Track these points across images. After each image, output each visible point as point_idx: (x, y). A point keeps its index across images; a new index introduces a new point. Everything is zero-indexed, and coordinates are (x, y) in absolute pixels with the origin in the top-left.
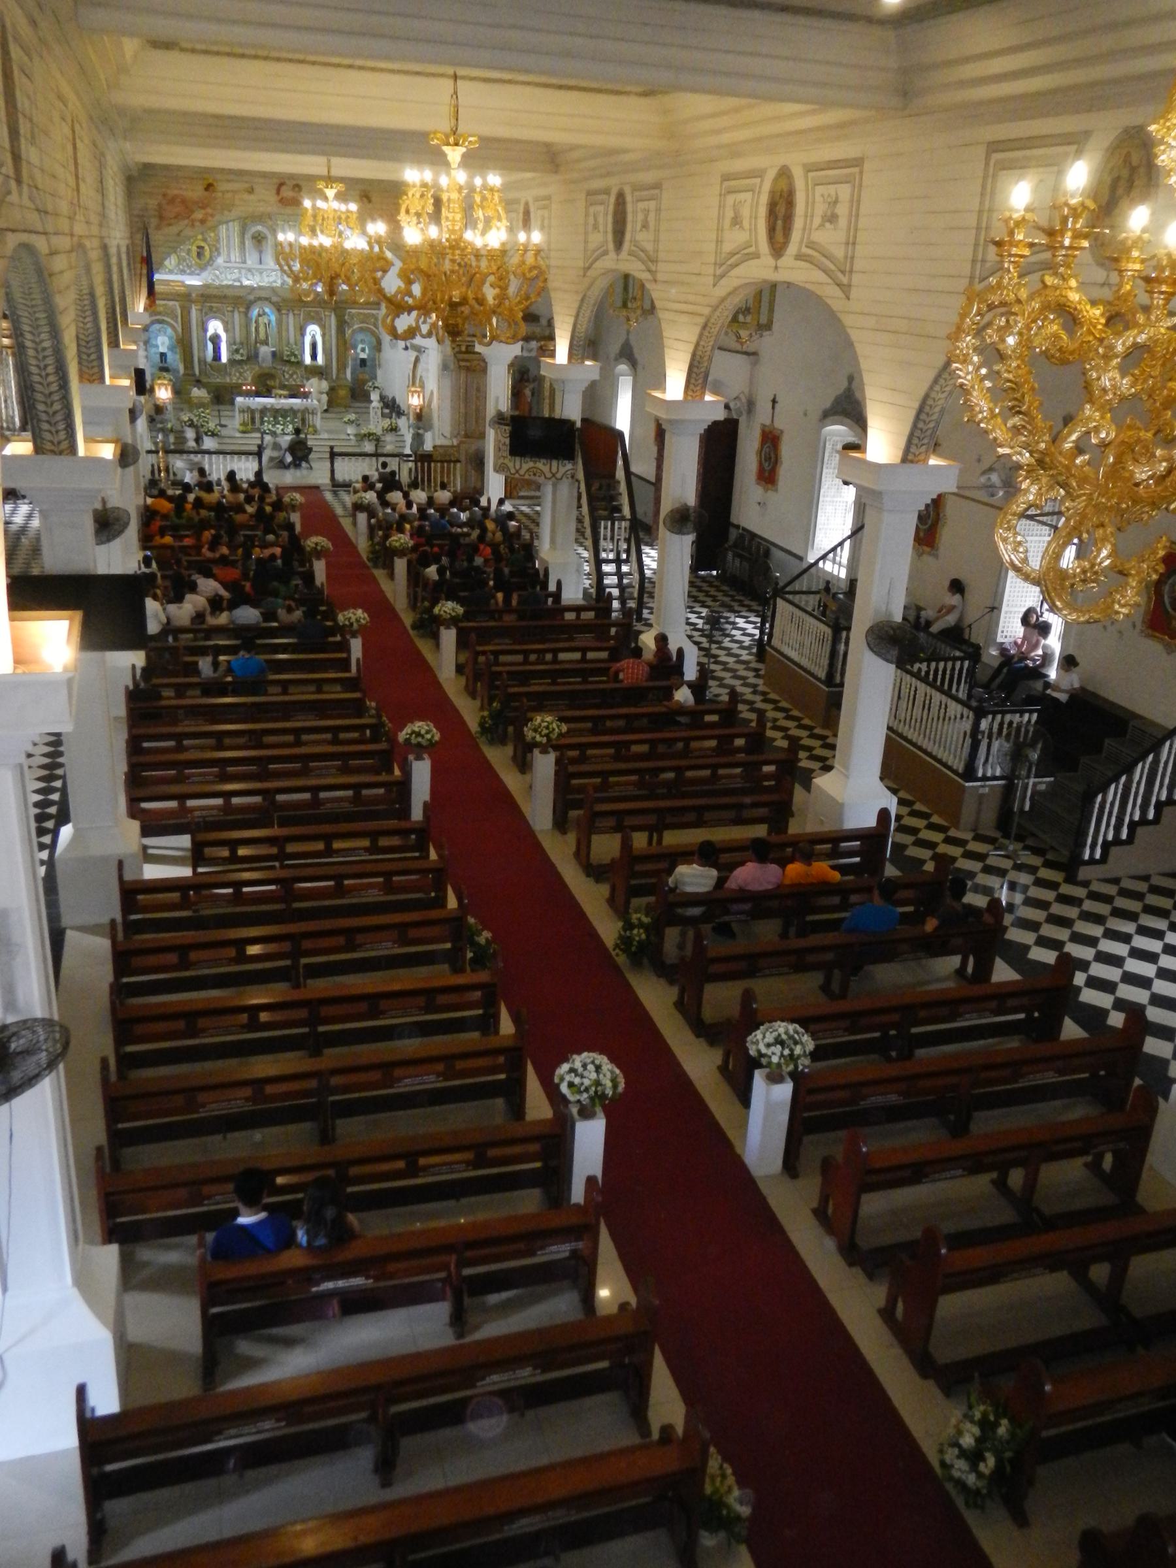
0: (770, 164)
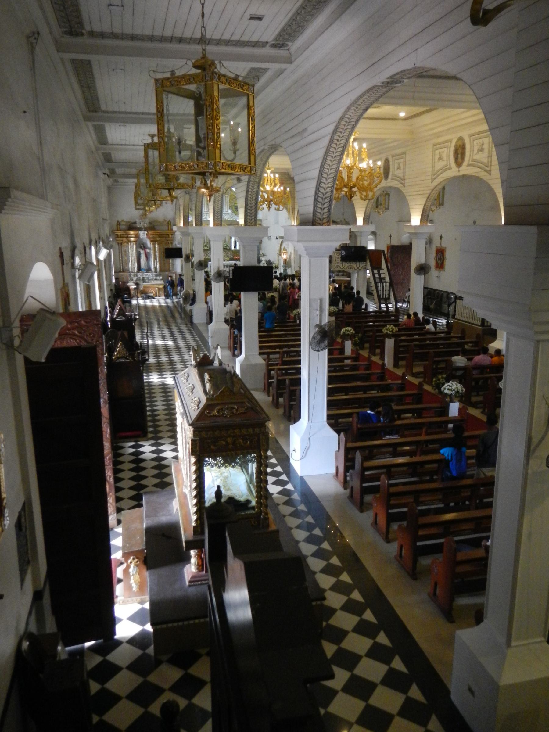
0: (454, 137)
